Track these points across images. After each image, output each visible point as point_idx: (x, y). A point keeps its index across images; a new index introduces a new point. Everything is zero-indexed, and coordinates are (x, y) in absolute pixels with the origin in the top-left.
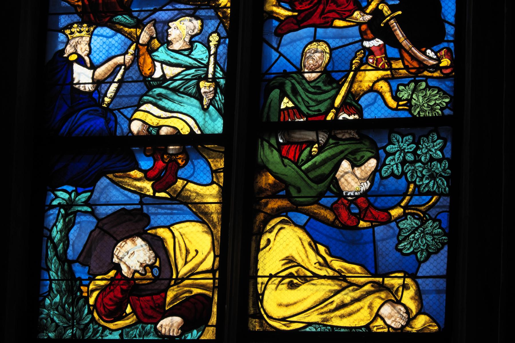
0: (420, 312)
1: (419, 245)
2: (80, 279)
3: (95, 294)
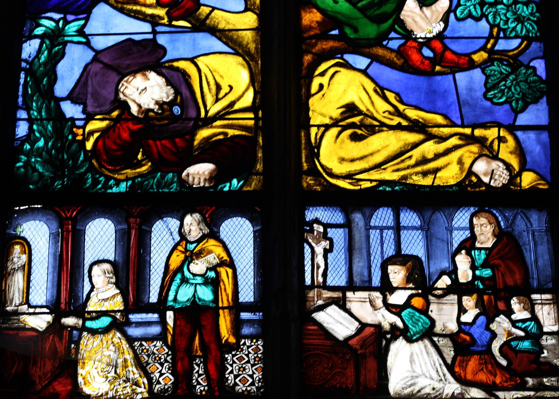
0: (523, 168)
1: (513, 93)
2: (73, 119)
3: (92, 140)
